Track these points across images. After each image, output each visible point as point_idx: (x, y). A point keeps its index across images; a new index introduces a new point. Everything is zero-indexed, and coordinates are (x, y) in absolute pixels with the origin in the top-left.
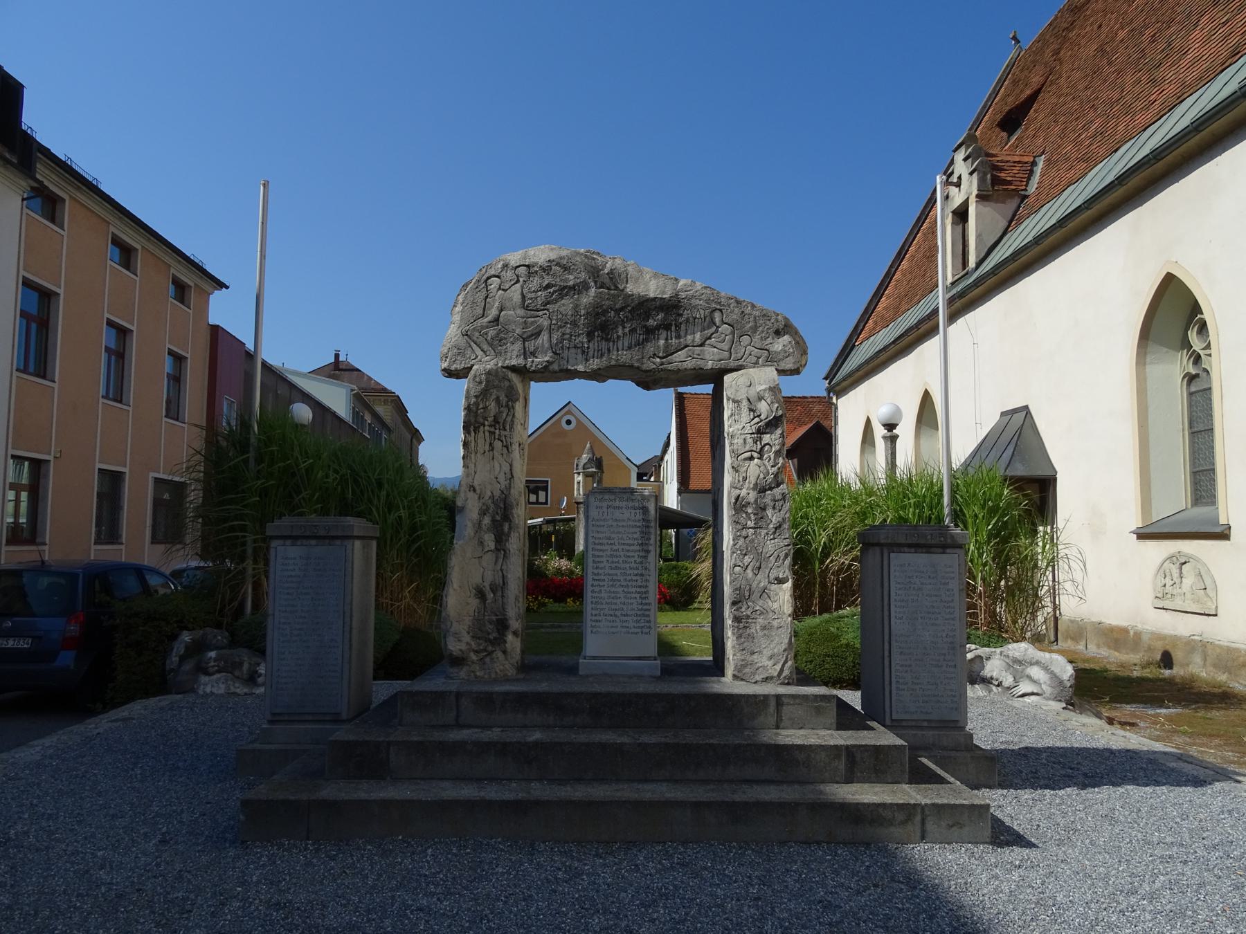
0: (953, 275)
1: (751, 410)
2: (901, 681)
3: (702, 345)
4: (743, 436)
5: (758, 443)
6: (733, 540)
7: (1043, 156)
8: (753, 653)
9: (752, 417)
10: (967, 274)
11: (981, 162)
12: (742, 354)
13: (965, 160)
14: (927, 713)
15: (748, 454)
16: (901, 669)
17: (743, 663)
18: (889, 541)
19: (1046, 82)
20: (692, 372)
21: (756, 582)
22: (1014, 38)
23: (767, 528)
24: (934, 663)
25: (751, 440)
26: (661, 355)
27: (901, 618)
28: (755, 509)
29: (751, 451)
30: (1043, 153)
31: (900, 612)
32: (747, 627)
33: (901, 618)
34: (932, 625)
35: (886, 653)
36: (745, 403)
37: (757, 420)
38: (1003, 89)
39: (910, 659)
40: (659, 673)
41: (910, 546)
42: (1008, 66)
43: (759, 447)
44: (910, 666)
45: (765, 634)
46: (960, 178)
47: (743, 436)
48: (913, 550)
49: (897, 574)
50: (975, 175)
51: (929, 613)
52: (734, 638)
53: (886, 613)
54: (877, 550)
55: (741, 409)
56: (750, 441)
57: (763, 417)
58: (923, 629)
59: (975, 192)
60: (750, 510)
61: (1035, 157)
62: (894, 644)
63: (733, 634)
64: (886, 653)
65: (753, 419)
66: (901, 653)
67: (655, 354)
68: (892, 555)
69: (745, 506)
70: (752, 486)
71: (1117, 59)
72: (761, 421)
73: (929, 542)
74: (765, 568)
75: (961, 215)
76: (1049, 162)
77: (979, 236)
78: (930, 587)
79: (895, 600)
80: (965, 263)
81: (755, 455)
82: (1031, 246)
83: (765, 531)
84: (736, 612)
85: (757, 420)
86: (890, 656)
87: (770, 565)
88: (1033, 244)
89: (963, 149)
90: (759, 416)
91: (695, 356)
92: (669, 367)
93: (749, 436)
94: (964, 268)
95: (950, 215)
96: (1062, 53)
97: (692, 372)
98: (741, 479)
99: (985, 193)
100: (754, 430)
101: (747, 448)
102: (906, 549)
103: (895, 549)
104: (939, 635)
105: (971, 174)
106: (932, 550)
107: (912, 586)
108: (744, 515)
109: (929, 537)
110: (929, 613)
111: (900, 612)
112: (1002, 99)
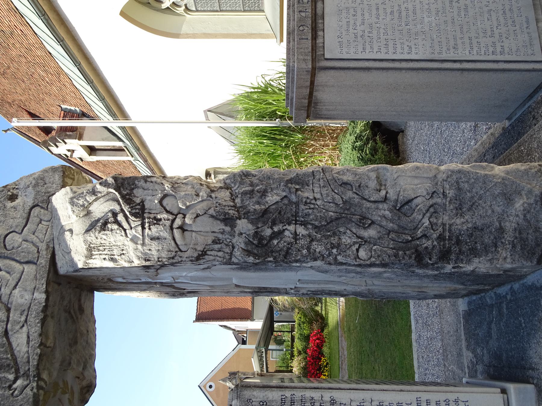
0: (128, 156)
1: (104, 227)
2: (491, 49)
3: (8, 310)
4: (147, 240)
5: (159, 217)
6: (315, 259)
7: (61, 106)
8: (501, 230)
9: (115, 227)
10: (126, 147)
11: (58, 137)
12: (30, 246)
13: (57, 146)
14: (528, 22)
15: (177, 233)
16: (475, 49)
17: (518, 248)
18: (309, 58)
19: (25, 109)
20: (51, 325)
21: (384, 223)
22: (6, 131)
23: (297, 204)
24: (463, 14)
25: (154, 229)
26: (11, 377)
27: (410, 48)
28: (265, 223)
29: (172, 228)
30: (60, 106)
31: (403, 49)
32: (457, 237)
33: (410, 48)
34: (415, 13)
35: (457, 66)
36: (92, 237)
37: (120, 218)
38: (34, 137)
39: (462, 38)
40: (530, 388)
41: (314, 37)
42: (21, 135)
43: (165, 216)
44: (470, 39)
45: (469, 209)
46: (69, 150)
47: (147, 240)
48: (320, 33)
49: (352, 50)
50: (66, 140)
51: (400, 17)
52: (476, 260)
53: (404, 65)
54: (322, 78)
55: (101, 245)
56: (155, 230)
57: (117, 208)
58: (421, 24)
59: (77, 141)
60: (268, 232)
61: (62, 110)
62: (444, 56)
63: (469, 262)
64: (457, 66)
65: (120, 225)
66: (454, 48)
67: (10, 387)
68: (327, 56)
69: (261, 239)
70: (228, 229)
71: (6, 63)
72: (122, 211)
73: (309, 14)
74: (360, 206)
75: (92, 150)
76: (64, 102)
77: (103, 140)
78: (367, 16)
79: (386, 53)
80: (120, 150)
81: (178, 222)
82: (105, 103)
83: (302, 207)
84: (434, 258)
85: (120, 218)
86: (461, 61)
87: (357, 199)
88: (104, 101)
89: (50, 148)
90: (115, 215)
91: (23, 318)
92: (34, 362)
93: (147, 230)
94: (123, 150)
95: (91, 156)
96: (9, 101)
97: (51, 325)
98: (217, 247)
99: (78, 136)
100: (135, 222)
101: (165, 234)
102: (319, 41)
103: (319, 53)
104: (426, 7)
105: (66, 143)
106: (319, 11)
107: (366, 34)
108: (275, 242)
109: (303, 14)
110: (400, 17)
111: (403, 49)
112: (38, 137)
